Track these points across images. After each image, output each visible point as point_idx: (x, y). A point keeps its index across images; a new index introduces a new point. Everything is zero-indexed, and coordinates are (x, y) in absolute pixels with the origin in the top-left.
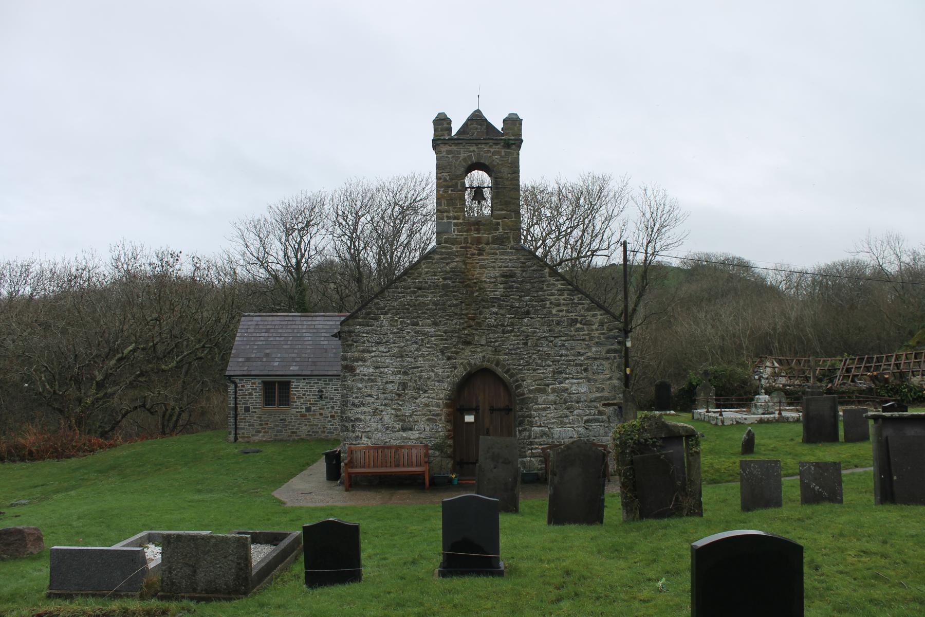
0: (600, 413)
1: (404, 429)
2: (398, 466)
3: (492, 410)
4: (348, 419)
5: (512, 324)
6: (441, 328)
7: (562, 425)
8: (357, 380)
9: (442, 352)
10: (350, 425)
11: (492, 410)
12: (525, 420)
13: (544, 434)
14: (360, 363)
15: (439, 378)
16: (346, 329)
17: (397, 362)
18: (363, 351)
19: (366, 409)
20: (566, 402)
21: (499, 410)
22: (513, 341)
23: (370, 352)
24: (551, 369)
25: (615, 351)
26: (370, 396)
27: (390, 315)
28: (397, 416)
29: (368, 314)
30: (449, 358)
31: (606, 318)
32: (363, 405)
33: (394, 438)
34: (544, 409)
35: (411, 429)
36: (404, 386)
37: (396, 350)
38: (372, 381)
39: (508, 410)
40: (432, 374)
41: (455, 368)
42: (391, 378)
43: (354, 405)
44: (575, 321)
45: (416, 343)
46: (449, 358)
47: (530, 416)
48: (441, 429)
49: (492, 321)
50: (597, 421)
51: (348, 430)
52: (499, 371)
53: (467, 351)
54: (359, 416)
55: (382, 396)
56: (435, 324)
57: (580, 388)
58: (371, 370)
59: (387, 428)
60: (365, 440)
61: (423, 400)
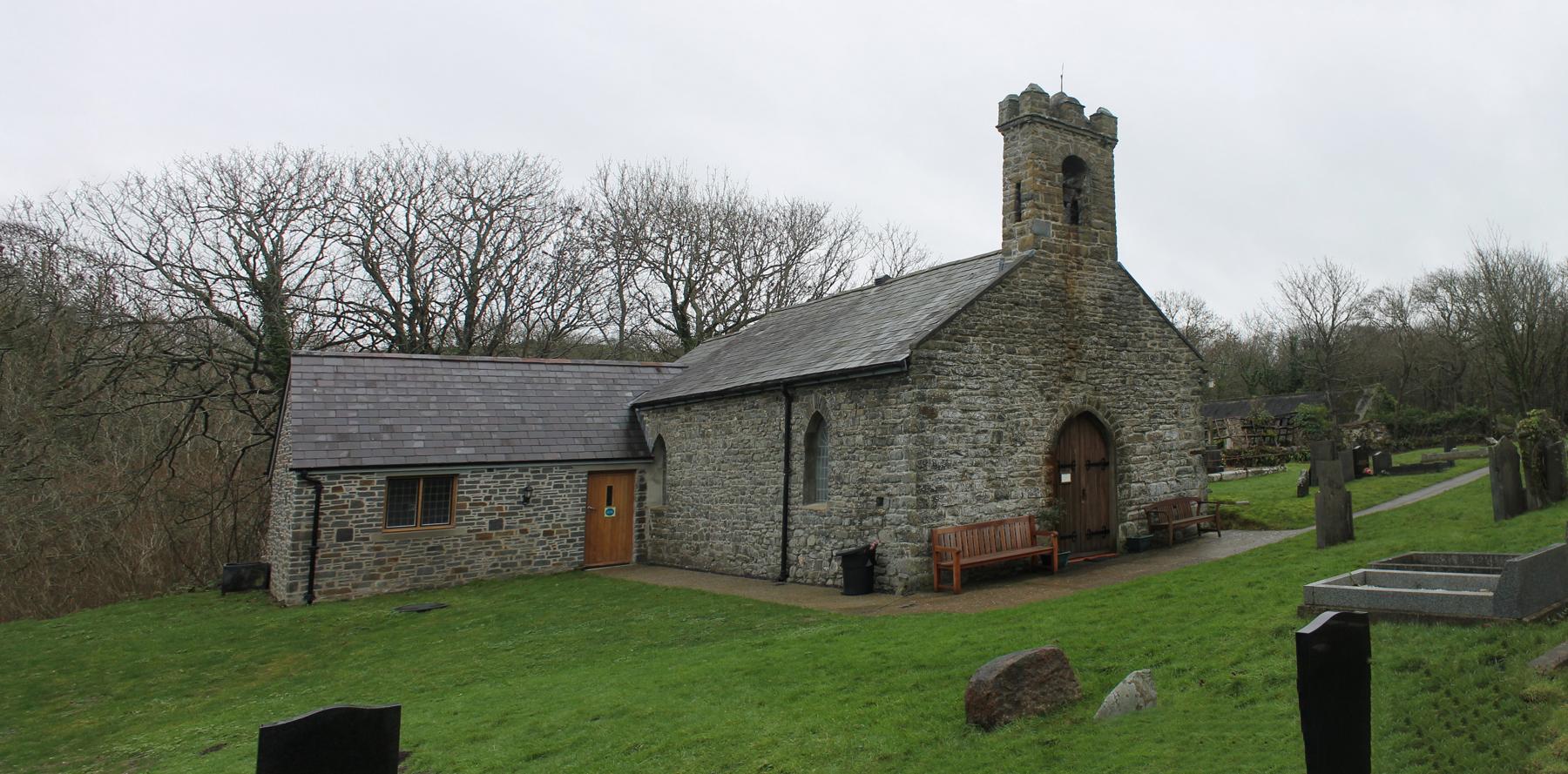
0: (1189, 463)
1: (998, 498)
2: (999, 550)
3: (1089, 465)
4: (927, 489)
5: (1111, 358)
6: (1040, 358)
7: (1157, 478)
8: (940, 430)
9: (1041, 390)
10: (929, 498)
11: (1089, 465)
12: (1122, 476)
13: (1143, 491)
14: (943, 404)
15: (1038, 423)
16: (924, 353)
17: (989, 403)
18: (947, 387)
19: (952, 472)
20: (1159, 453)
21: (1096, 465)
22: (1112, 378)
23: (956, 388)
24: (1147, 412)
25: (1198, 392)
26: (957, 453)
27: (980, 338)
28: (989, 480)
29: (954, 333)
30: (1049, 399)
31: (1191, 356)
32: (948, 465)
33: (986, 512)
34: (1142, 461)
35: (1007, 498)
36: (999, 435)
37: (990, 386)
38: (960, 430)
39: (1105, 464)
40: (1030, 419)
41: (1055, 411)
42: (984, 425)
43: (935, 466)
44: (1167, 357)
45: (1012, 377)
46: (1049, 399)
47: (1129, 470)
48: (1041, 493)
49: (1092, 352)
50: (1186, 471)
51: (927, 506)
52: (1100, 414)
53: (1068, 387)
54: (942, 483)
55: (972, 452)
56: (1034, 353)
57: (1172, 435)
58: (959, 414)
59: (979, 498)
60: (949, 519)
61: (1019, 456)
